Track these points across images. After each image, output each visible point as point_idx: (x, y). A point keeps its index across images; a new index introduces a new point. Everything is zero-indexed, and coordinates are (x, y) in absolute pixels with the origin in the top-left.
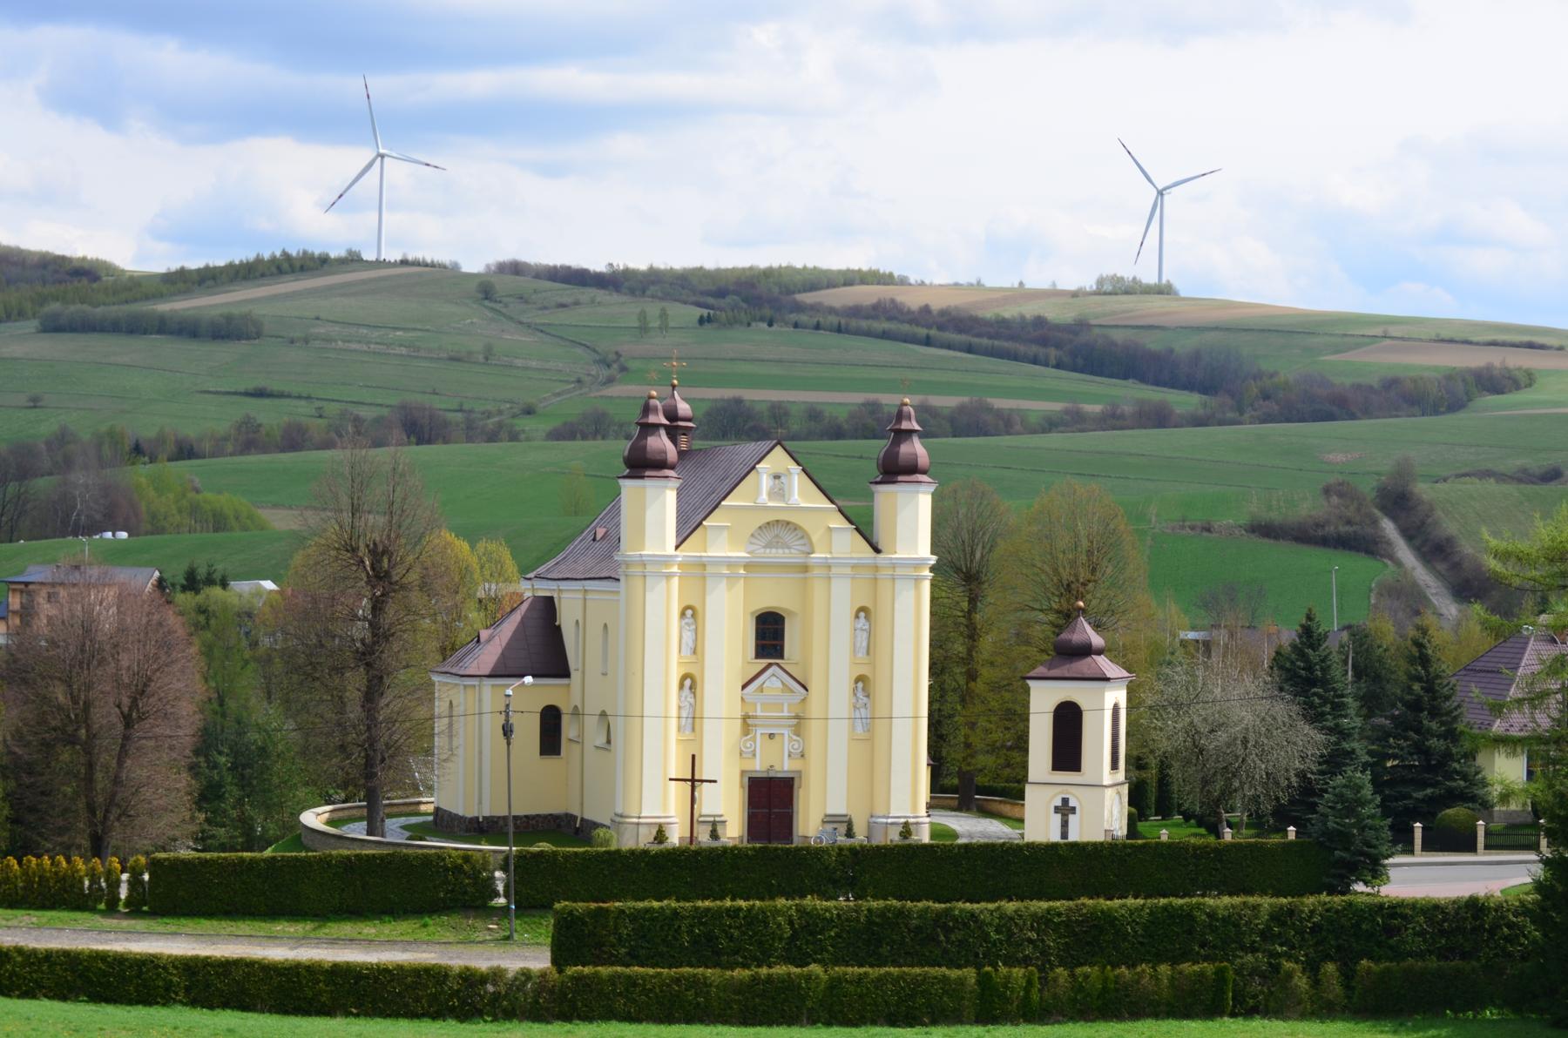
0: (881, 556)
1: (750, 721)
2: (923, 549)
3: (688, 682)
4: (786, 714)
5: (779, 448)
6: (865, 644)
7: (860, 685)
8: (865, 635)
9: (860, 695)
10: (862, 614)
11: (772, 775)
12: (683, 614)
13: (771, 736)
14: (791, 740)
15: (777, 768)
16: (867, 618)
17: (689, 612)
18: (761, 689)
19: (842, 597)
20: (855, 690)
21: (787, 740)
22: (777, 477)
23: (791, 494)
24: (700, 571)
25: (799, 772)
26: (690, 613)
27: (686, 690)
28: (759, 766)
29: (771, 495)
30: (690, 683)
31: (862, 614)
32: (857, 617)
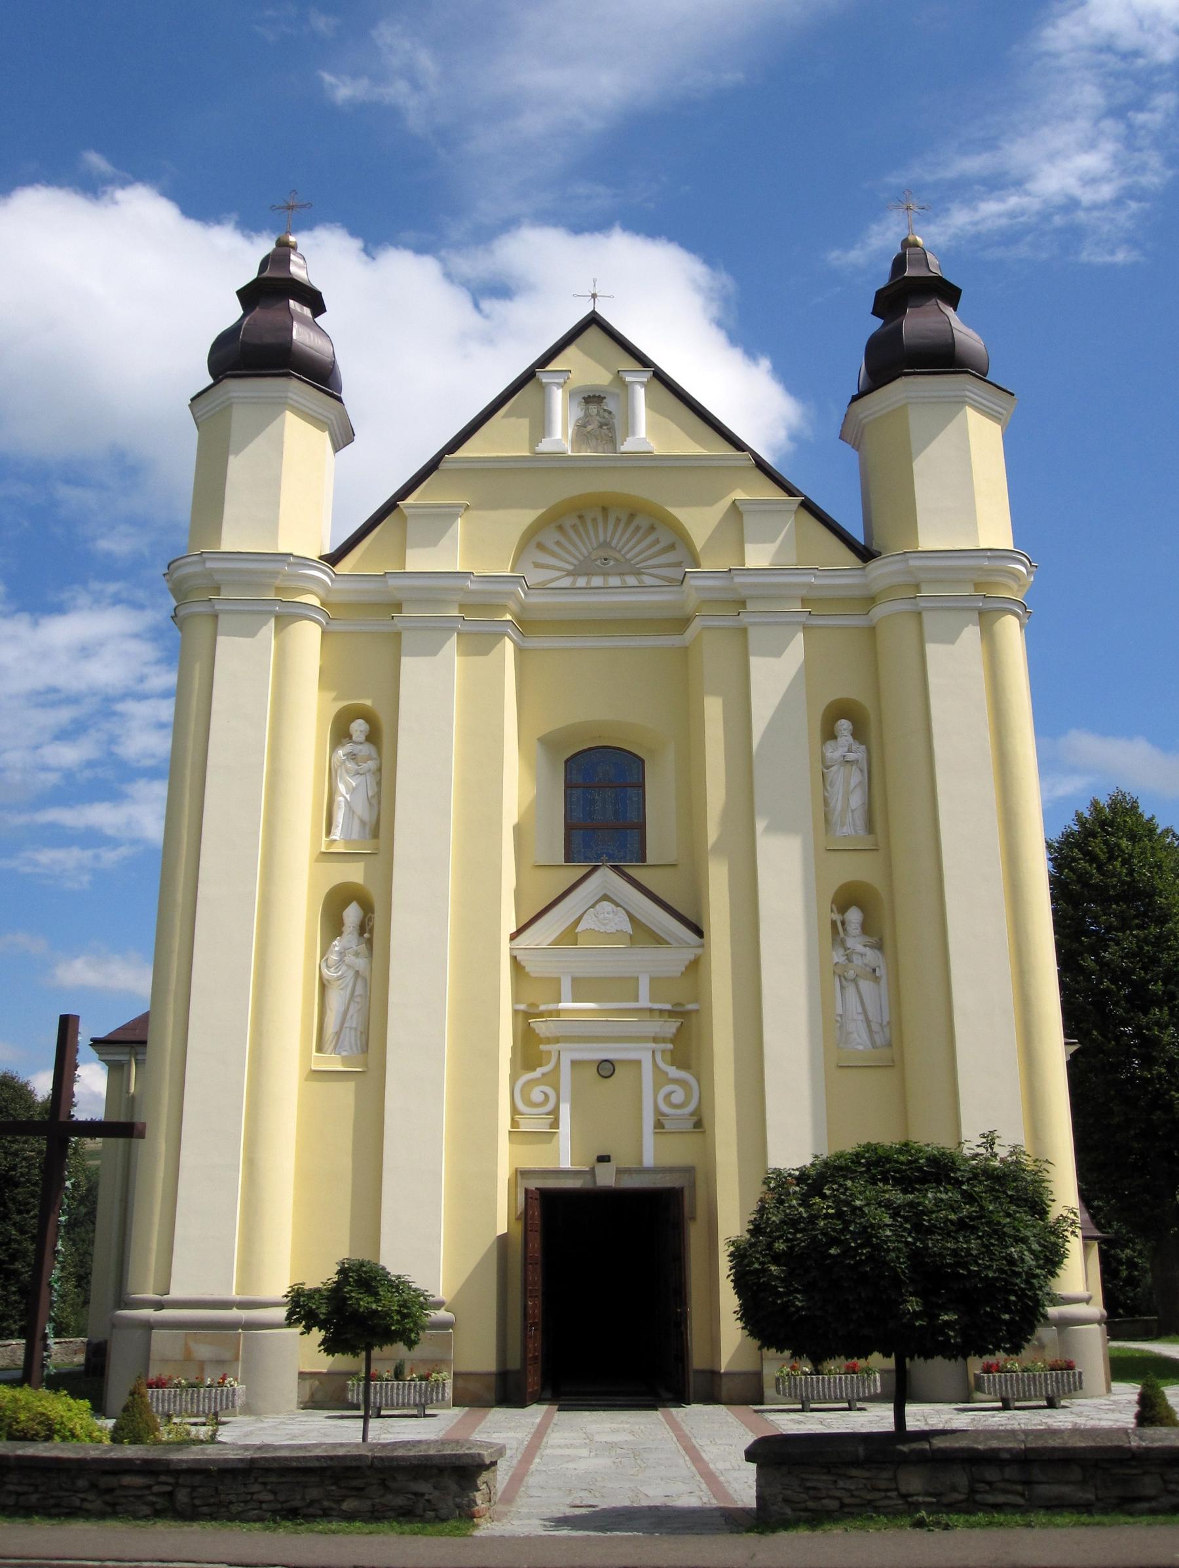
0: (873, 565)
1: (541, 1027)
2: (994, 529)
3: (352, 914)
4: (644, 1002)
5: (593, 333)
6: (857, 800)
7: (854, 916)
8: (856, 777)
9: (856, 943)
10: (844, 725)
11: (606, 1178)
12: (340, 733)
13: (606, 1068)
14: (661, 1078)
15: (623, 1158)
16: (859, 734)
17: (359, 728)
18: (570, 935)
19: (777, 674)
20: (837, 931)
21: (653, 1088)
22: (592, 399)
23: (629, 428)
24: (379, 622)
25: (689, 1171)
26: (365, 730)
27: (349, 938)
28: (563, 1156)
29: (582, 433)
30: (356, 914)
31: (844, 725)
32: (830, 734)
